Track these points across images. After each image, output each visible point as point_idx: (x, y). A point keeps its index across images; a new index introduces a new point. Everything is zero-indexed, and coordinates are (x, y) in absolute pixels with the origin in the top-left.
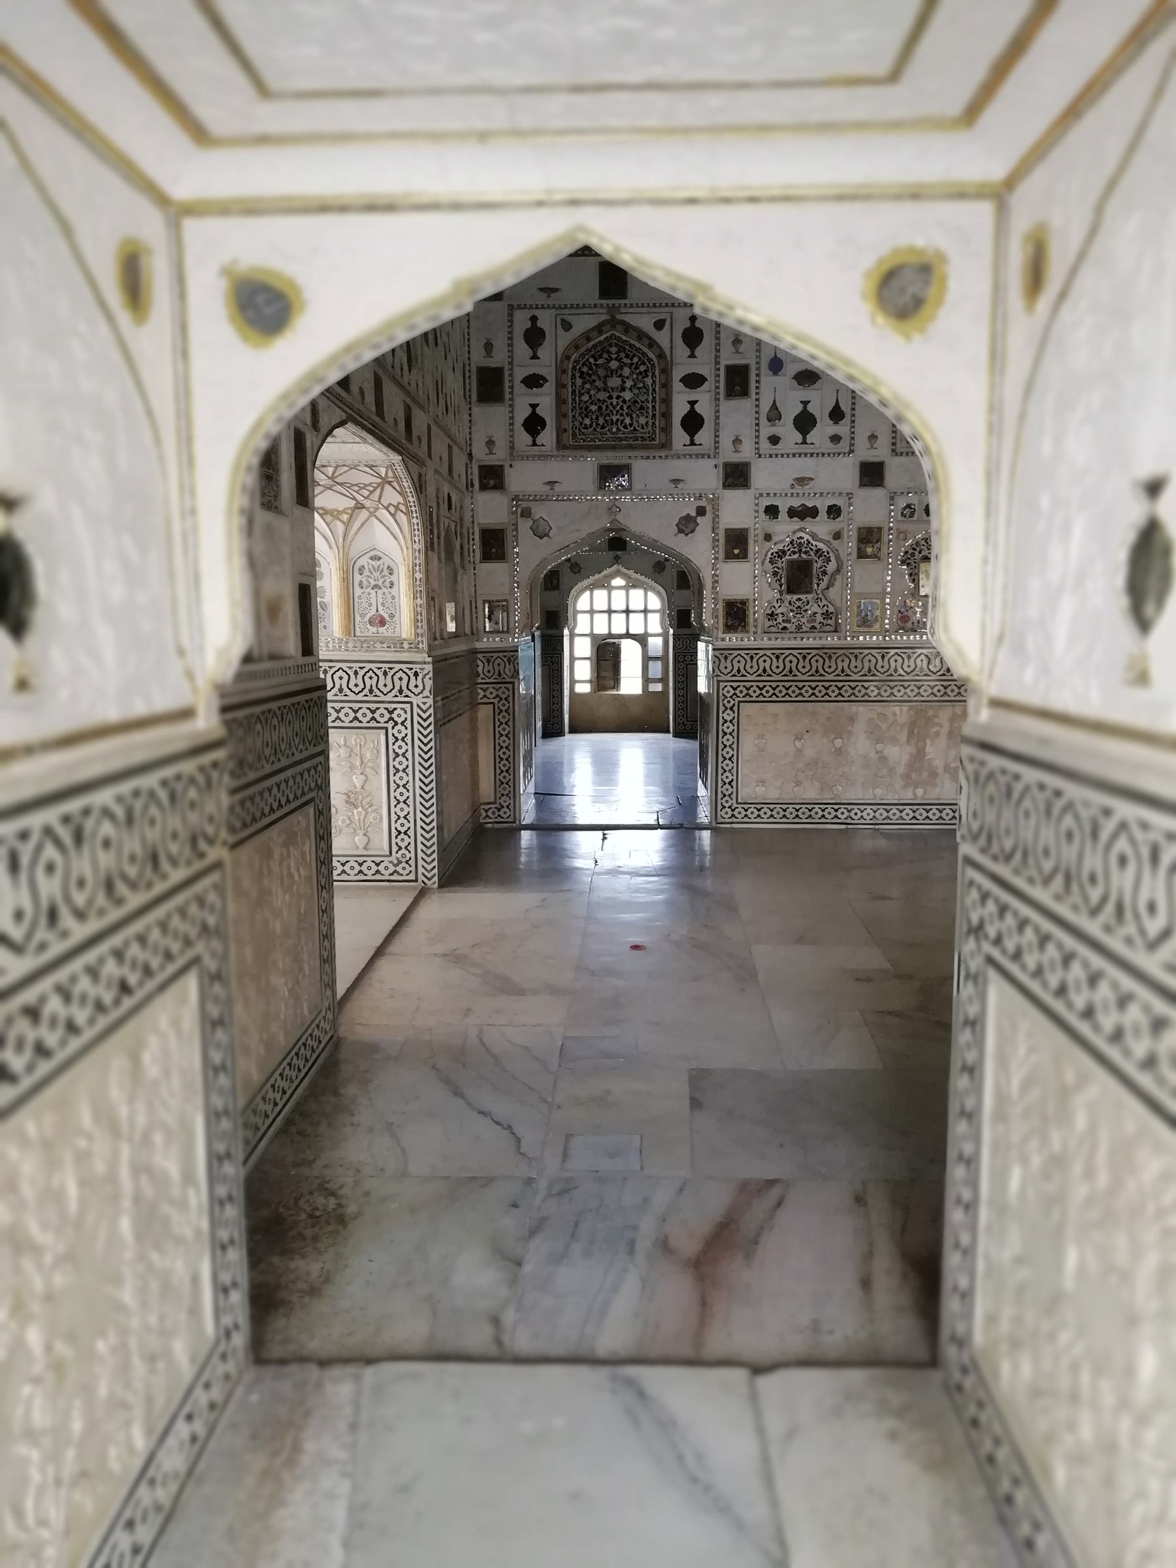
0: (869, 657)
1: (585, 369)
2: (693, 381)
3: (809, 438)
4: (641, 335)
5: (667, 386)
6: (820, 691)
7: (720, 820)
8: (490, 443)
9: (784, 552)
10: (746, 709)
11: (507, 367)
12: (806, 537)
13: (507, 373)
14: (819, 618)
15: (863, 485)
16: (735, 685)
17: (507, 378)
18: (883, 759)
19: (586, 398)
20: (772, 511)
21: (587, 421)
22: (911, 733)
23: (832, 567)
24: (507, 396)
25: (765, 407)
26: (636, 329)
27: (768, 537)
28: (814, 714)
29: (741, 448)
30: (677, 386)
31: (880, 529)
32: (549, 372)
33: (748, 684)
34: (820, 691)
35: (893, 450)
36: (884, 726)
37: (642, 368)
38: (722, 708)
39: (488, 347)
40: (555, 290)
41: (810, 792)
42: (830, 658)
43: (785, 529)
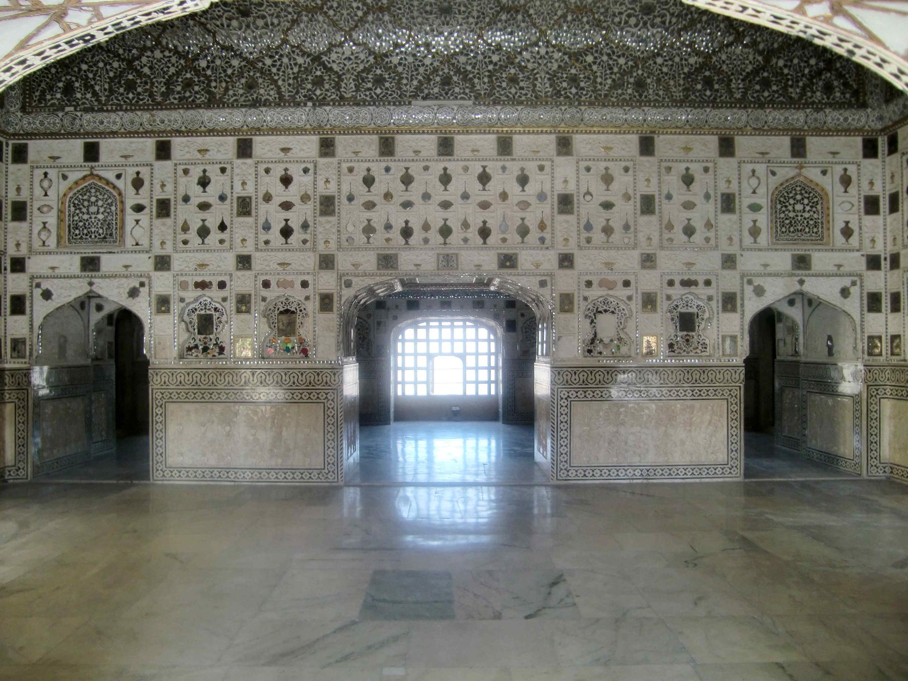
1: (76, 202)
3: (206, 241)
4: (108, 183)
5: (123, 211)
8: (18, 245)
10: (171, 407)
12: (209, 300)
13: (29, 204)
15: (238, 269)
19: (76, 218)
20: (184, 286)
23: (224, 319)
25: (180, 223)
26: (104, 179)
30: (129, 211)
31: (250, 295)
35: (257, 248)
36: (255, 418)
37: (110, 201)
38: (155, 406)
39: (18, 189)
40: (58, 158)
41: (212, 461)
43: (191, 294)
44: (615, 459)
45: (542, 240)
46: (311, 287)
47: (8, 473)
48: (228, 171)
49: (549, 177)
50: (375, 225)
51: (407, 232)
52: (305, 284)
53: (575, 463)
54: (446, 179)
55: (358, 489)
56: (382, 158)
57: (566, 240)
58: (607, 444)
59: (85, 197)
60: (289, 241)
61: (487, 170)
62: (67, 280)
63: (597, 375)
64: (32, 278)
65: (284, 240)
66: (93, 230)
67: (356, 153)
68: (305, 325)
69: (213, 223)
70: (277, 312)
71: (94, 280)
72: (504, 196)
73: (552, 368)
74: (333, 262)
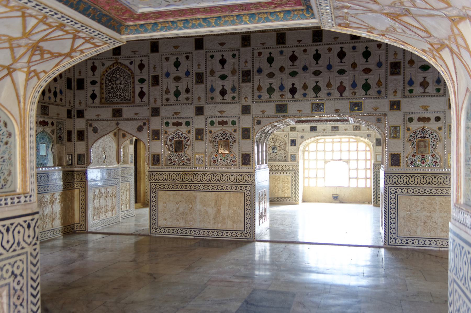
0: (200, 175)
1: (109, 78)
2: (142, 81)
4: (126, 67)
5: (134, 83)
6: (184, 187)
7: (152, 233)
8: (80, 103)
9: (173, 138)
10: (160, 193)
11: (85, 78)
13: (85, 80)
14: (185, 161)
16: (156, 184)
17: (85, 82)
18: (206, 212)
19: (110, 87)
20: (167, 124)
21: (110, 95)
22: (216, 203)
23: (189, 143)
24: (85, 88)
25: (164, 89)
26: (124, 65)
27: (166, 133)
28: (182, 195)
29: (157, 102)
30: (137, 82)
31: (203, 130)
32: (98, 80)
33: (160, 184)
34: (184, 187)
35: (206, 102)
38: (151, 192)
41: (182, 224)
42: (187, 175)
43: (171, 129)
44: (429, 234)
45: (379, 92)
46: (237, 124)
47: (76, 227)
48: (190, 58)
49: (384, 51)
50: (274, 87)
51: (293, 91)
52: (234, 123)
53: (400, 234)
54: (317, 57)
55: (268, 244)
56: (278, 46)
57: (395, 92)
58: (423, 224)
59: (114, 75)
60: (225, 98)
61: (344, 50)
62: (106, 122)
63: (416, 179)
64: (87, 121)
65: (221, 97)
66: (118, 94)
67: (263, 44)
68: (234, 146)
69: (182, 89)
70: (218, 139)
71: (118, 122)
72: (354, 66)
73: (384, 173)
74: (249, 110)
